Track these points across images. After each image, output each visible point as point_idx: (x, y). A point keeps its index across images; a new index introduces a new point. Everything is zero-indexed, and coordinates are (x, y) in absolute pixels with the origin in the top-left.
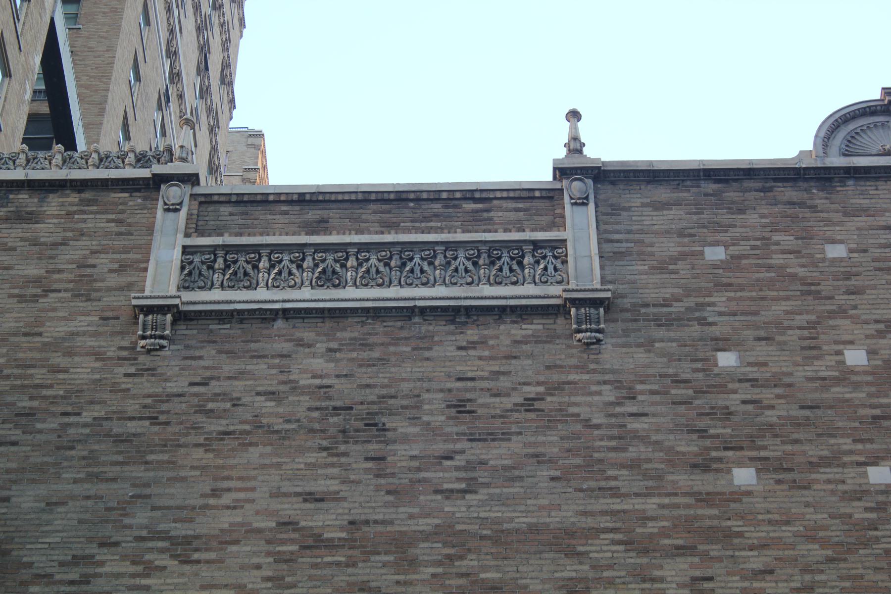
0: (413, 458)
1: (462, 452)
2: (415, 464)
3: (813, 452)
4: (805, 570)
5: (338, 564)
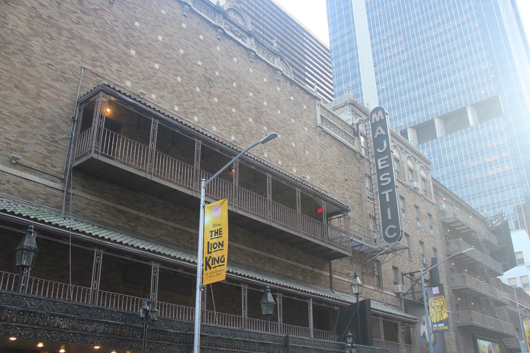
0: (67, 8)
1: (78, 13)
2: (67, 10)
3: (147, 54)
4: (138, 79)
5: (44, 25)
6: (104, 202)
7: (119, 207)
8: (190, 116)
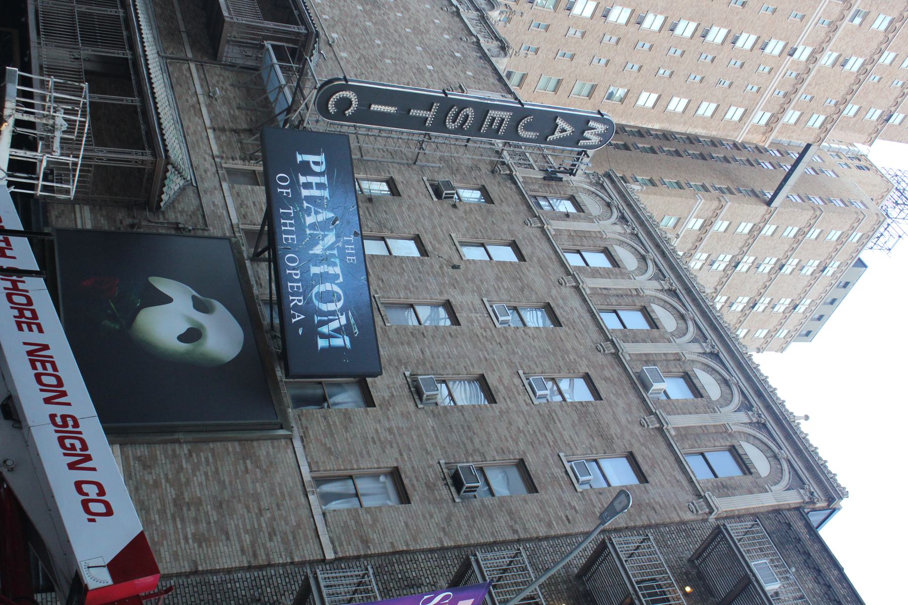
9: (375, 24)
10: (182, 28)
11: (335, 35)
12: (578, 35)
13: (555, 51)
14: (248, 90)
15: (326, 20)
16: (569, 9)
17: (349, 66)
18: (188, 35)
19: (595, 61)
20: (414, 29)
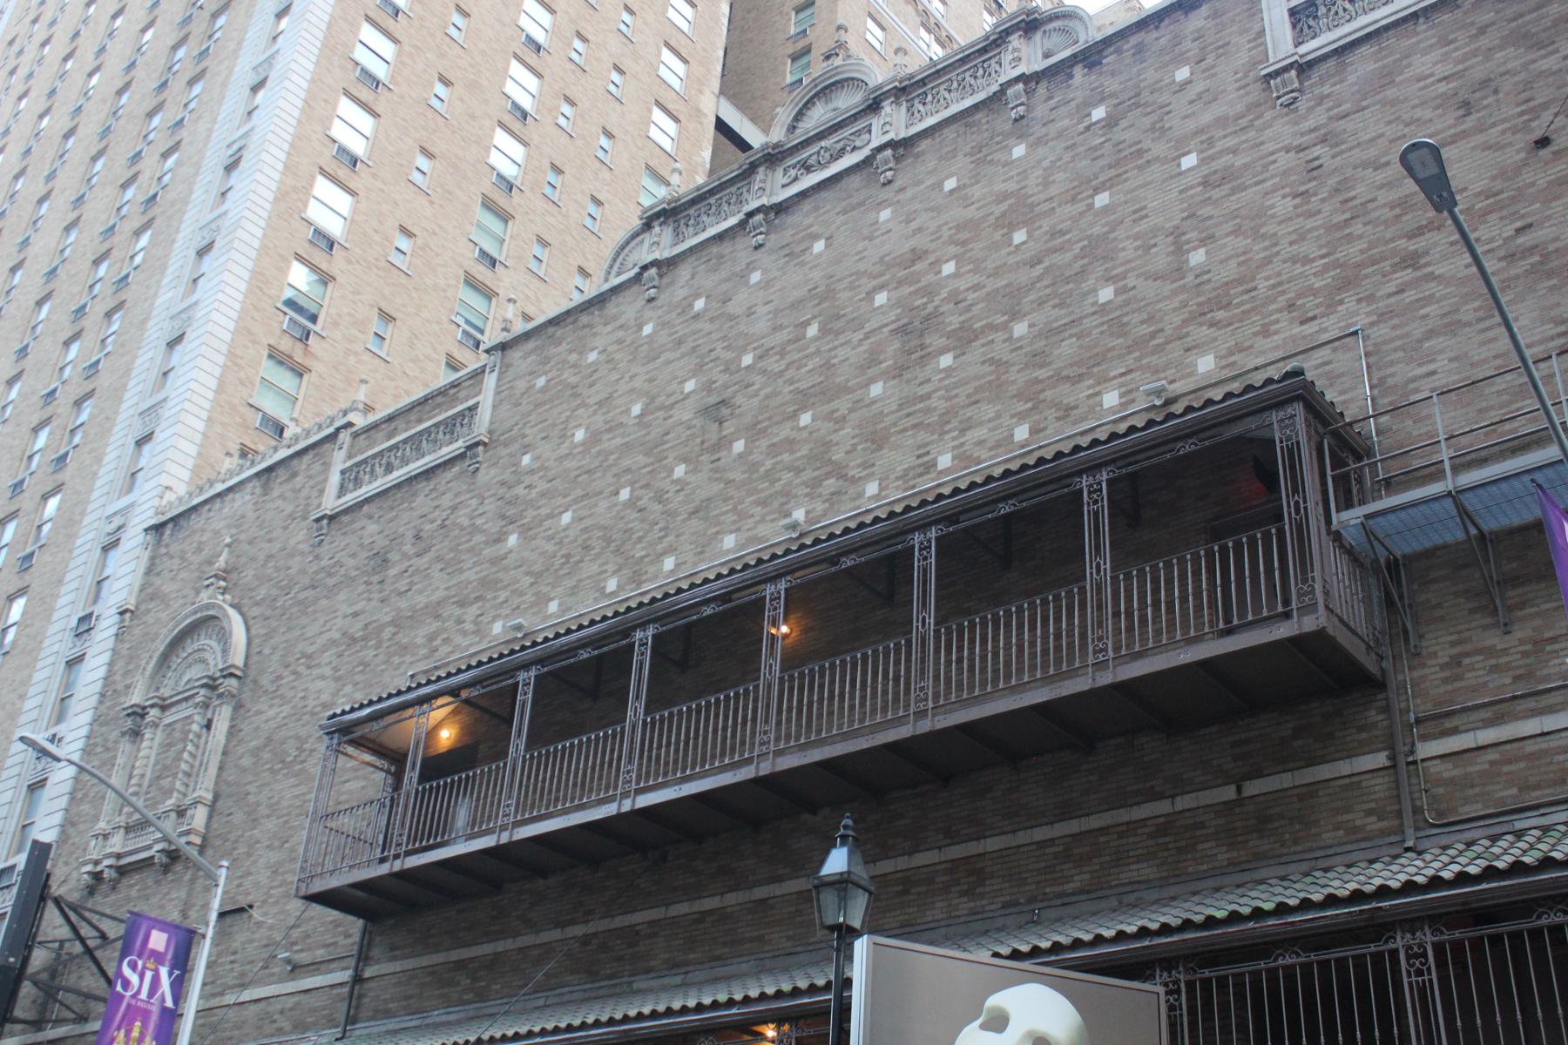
3: (544, 511)
6: (424, 961)
7: (455, 955)
8: (651, 570)
9: (1015, 316)
10: (1229, 793)
11: (1111, 399)
12: (566, 109)
13: (598, 165)
14: (1514, 581)
15: (1034, 431)
16: (525, 115)
17: (1262, 343)
18: (1258, 774)
19: (612, 88)
20: (1008, 224)
